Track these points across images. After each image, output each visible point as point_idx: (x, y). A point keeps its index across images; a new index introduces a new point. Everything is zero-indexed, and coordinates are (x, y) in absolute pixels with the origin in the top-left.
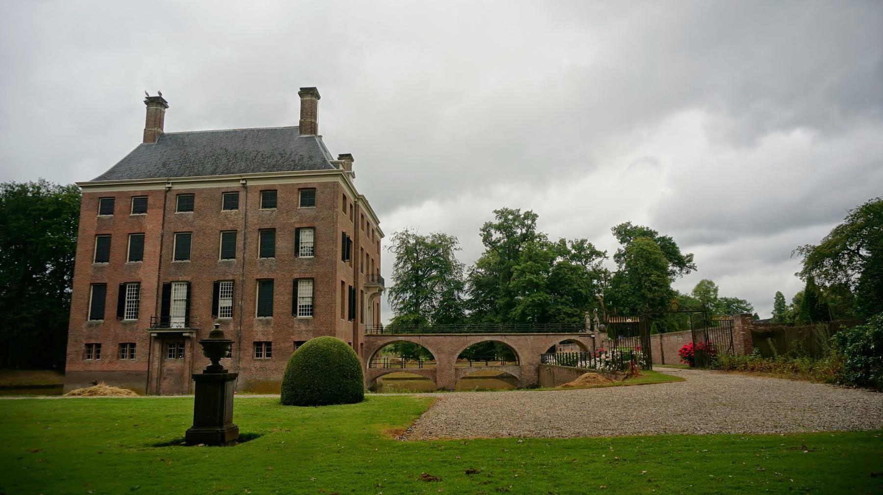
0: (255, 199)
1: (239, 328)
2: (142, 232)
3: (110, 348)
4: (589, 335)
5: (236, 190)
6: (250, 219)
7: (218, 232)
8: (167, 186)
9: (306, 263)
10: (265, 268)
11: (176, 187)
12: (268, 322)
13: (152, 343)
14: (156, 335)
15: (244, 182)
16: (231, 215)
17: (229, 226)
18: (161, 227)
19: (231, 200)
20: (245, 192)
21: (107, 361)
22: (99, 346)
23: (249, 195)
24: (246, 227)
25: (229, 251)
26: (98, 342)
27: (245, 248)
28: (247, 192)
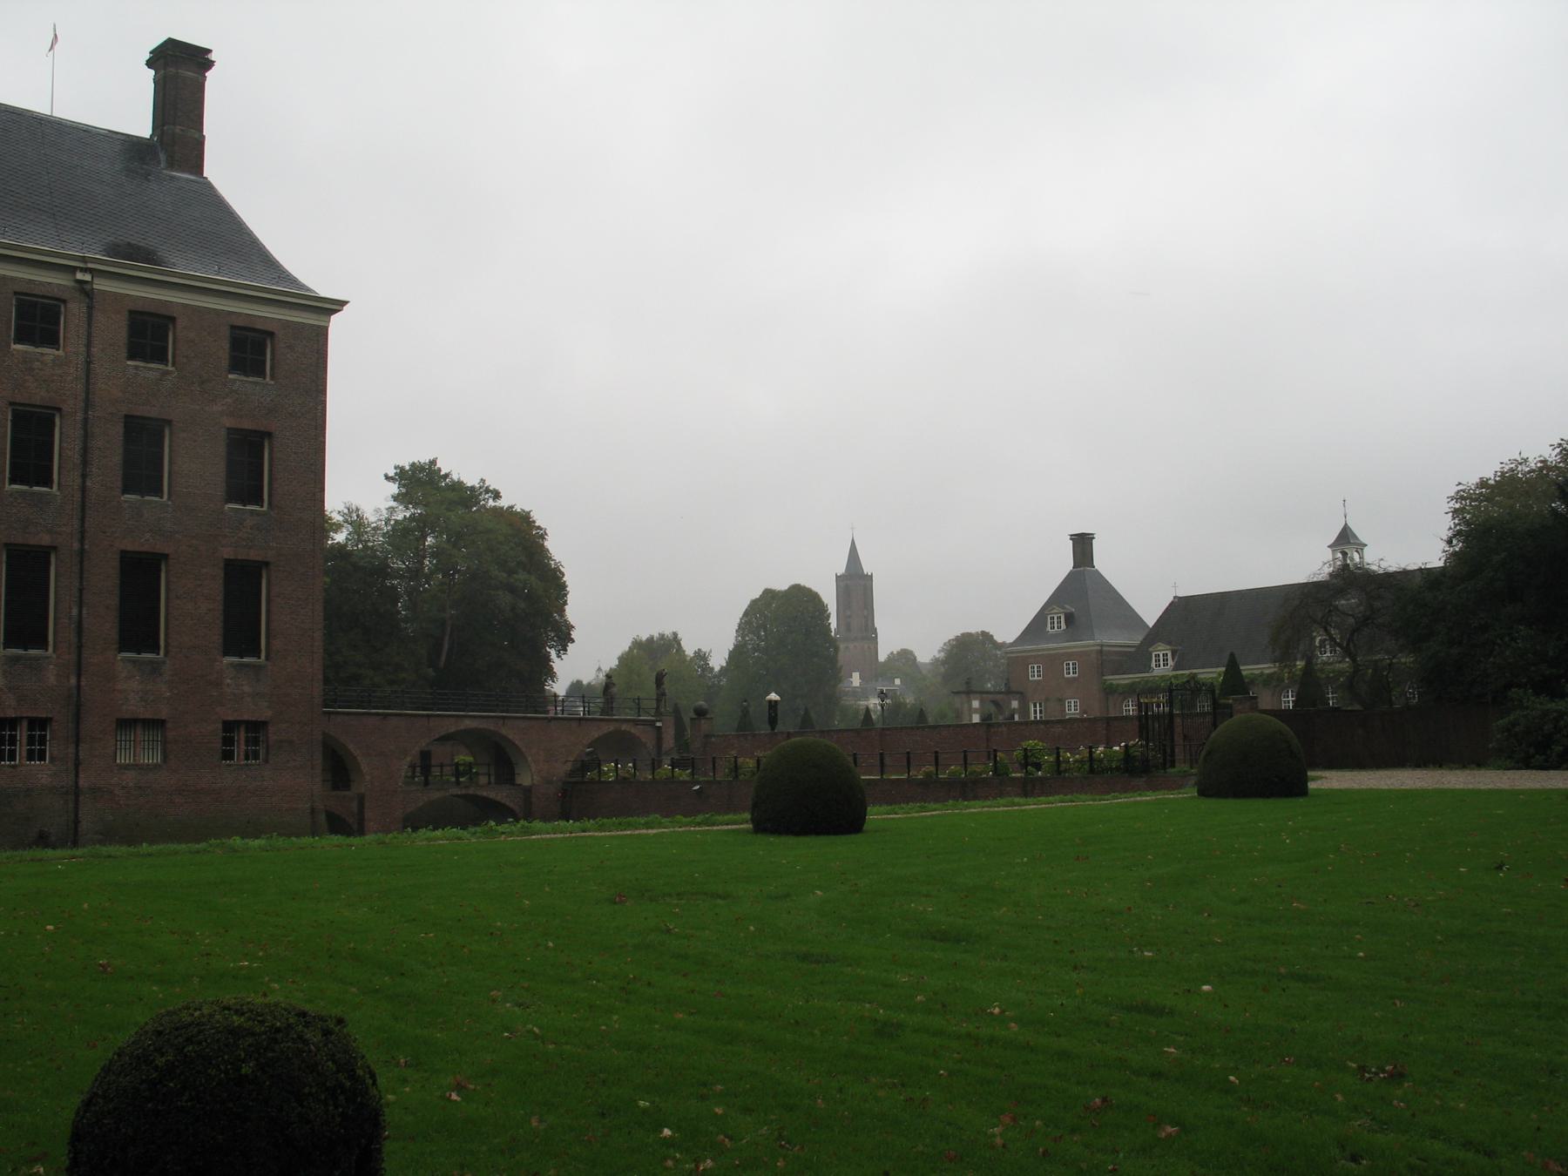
0: (112, 329)
1: (73, 681)
4: (652, 723)
15: (88, 277)
17: (37, 394)
27: (85, 462)
28: (90, 308)
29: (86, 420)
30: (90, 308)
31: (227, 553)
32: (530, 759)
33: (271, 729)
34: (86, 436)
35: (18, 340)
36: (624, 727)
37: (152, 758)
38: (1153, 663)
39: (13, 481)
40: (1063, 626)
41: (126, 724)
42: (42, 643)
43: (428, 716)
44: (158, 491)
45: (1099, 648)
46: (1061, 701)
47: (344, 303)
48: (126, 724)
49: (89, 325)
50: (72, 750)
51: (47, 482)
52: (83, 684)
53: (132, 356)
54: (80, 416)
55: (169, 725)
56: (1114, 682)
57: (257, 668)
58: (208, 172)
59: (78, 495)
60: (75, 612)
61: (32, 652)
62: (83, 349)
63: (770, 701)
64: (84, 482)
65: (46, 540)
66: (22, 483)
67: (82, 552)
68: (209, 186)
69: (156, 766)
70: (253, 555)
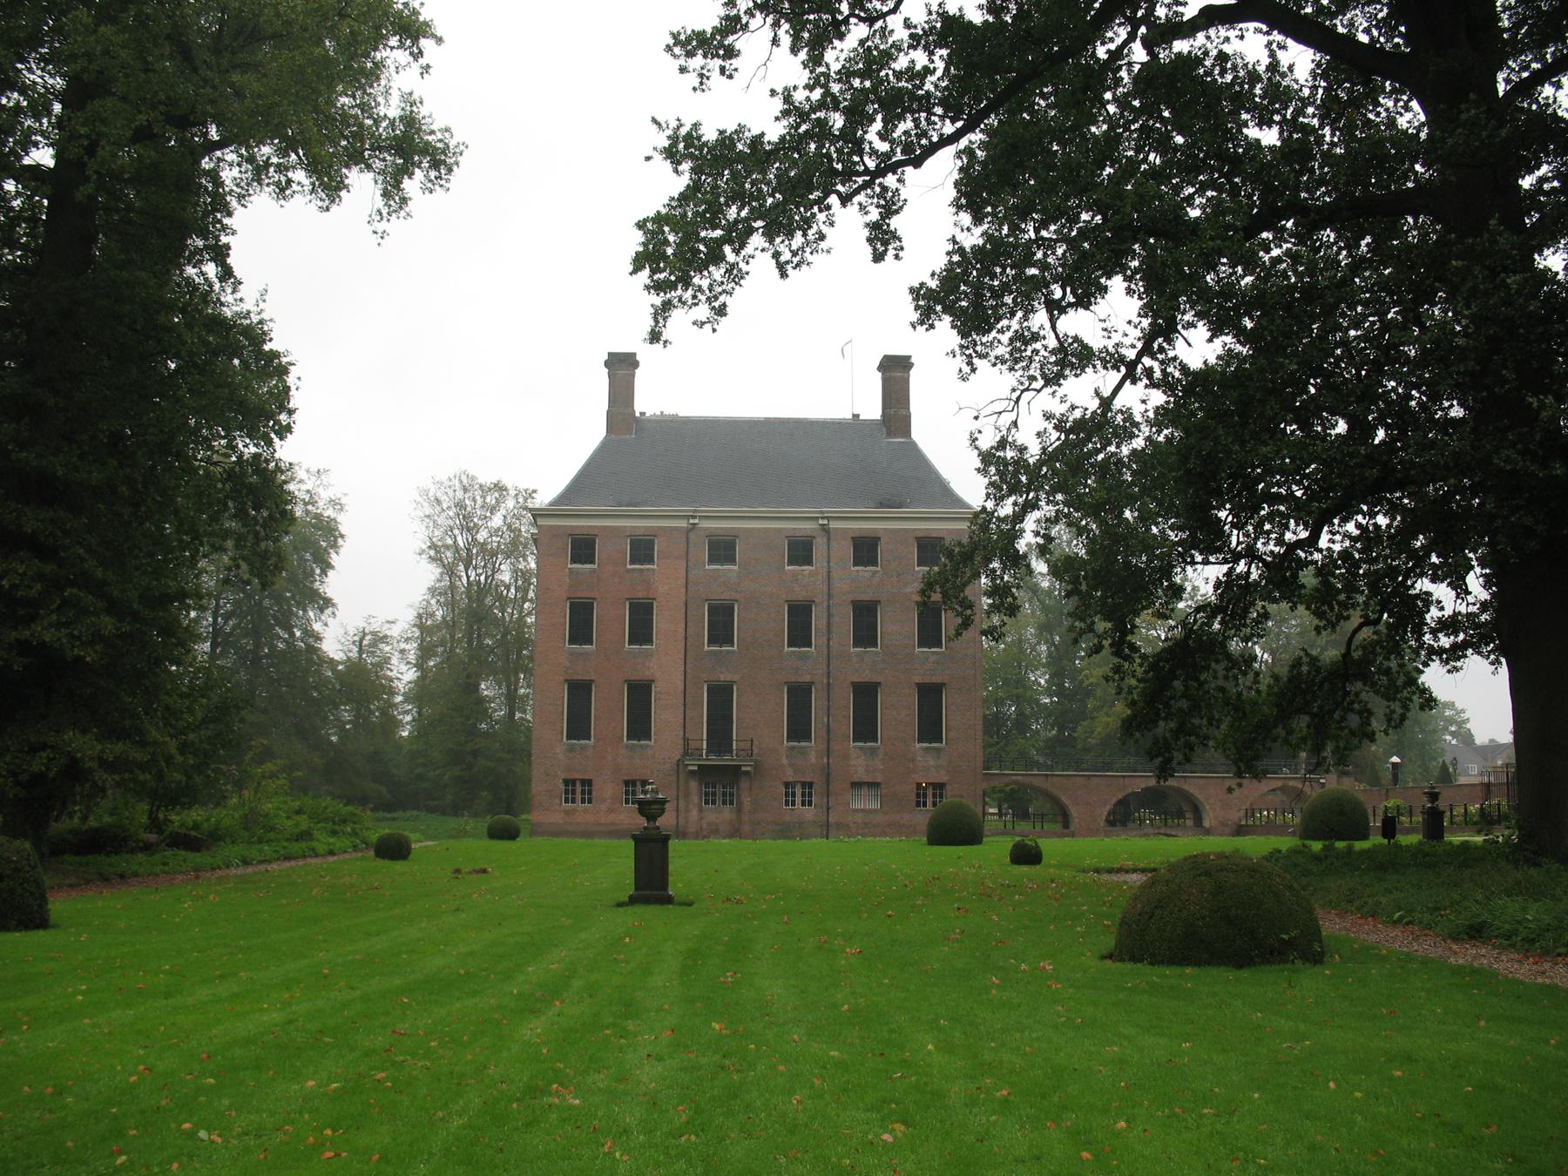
1: (825, 760)
2: (651, 596)
5: (809, 533)
8: (691, 521)
9: (933, 658)
10: (861, 664)
11: (706, 524)
12: (873, 751)
13: (682, 782)
14: (696, 768)
15: (826, 522)
16: (804, 576)
17: (800, 594)
18: (683, 590)
19: (801, 551)
20: (825, 540)
21: (604, 807)
22: (587, 783)
23: (834, 544)
24: (830, 596)
25: (800, 633)
27: (829, 632)
28: (829, 539)
29: (829, 606)
30: (829, 539)
31: (918, 679)
32: (1208, 807)
33: (948, 787)
34: (829, 616)
35: (790, 563)
36: (1291, 783)
37: (874, 805)
39: (790, 645)
41: (856, 785)
42: (808, 737)
43: (1123, 776)
44: (876, 645)
48: (856, 785)
49: (829, 547)
50: (825, 800)
51: (810, 645)
53: (855, 564)
54: (826, 603)
55: (883, 786)
57: (938, 750)
58: (917, 434)
59: (826, 650)
60: (826, 720)
61: (803, 744)
62: (825, 564)
63: (1393, 764)
65: (808, 678)
66: (795, 646)
67: (829, 684)
68: (914, 445)
69: (875, 810)
70: (935, 679)
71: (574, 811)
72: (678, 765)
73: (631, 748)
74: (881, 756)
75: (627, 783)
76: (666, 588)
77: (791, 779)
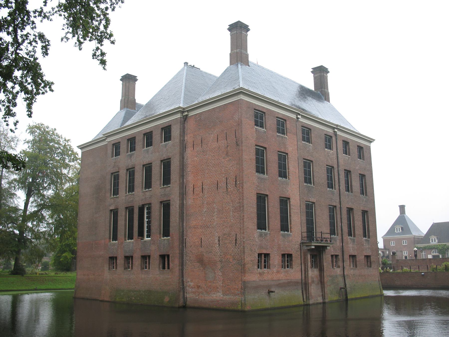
1: (341, 244)
3: (276, 260)
6: (340, 161)
7: (325, 165)
26: (265, 252)
33: (371, 258)
38: (431, 241)
40: (401, 231)
45: (414, 237)
46: (401, 251)
47: (374, 140)
52: (344, 245)
56: (419, 246)
62: (336, 150)
64: (339, 188)
71: (264, 273)
72: (300, 246)
73: (284, 236)
74: (356, 243)
75: (283, 255)
76: (291, 149)
77: (333, 254)
